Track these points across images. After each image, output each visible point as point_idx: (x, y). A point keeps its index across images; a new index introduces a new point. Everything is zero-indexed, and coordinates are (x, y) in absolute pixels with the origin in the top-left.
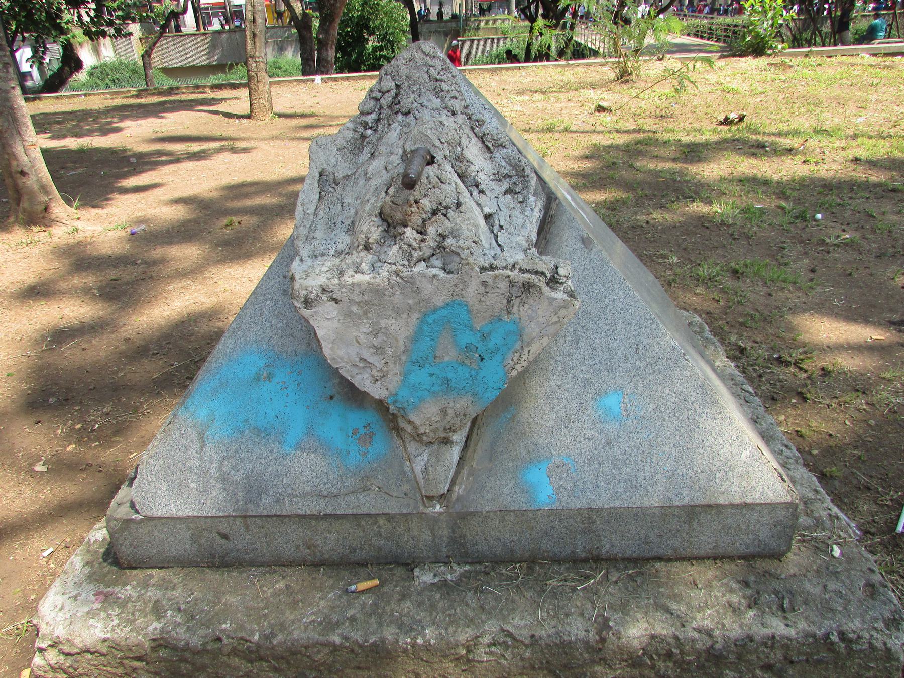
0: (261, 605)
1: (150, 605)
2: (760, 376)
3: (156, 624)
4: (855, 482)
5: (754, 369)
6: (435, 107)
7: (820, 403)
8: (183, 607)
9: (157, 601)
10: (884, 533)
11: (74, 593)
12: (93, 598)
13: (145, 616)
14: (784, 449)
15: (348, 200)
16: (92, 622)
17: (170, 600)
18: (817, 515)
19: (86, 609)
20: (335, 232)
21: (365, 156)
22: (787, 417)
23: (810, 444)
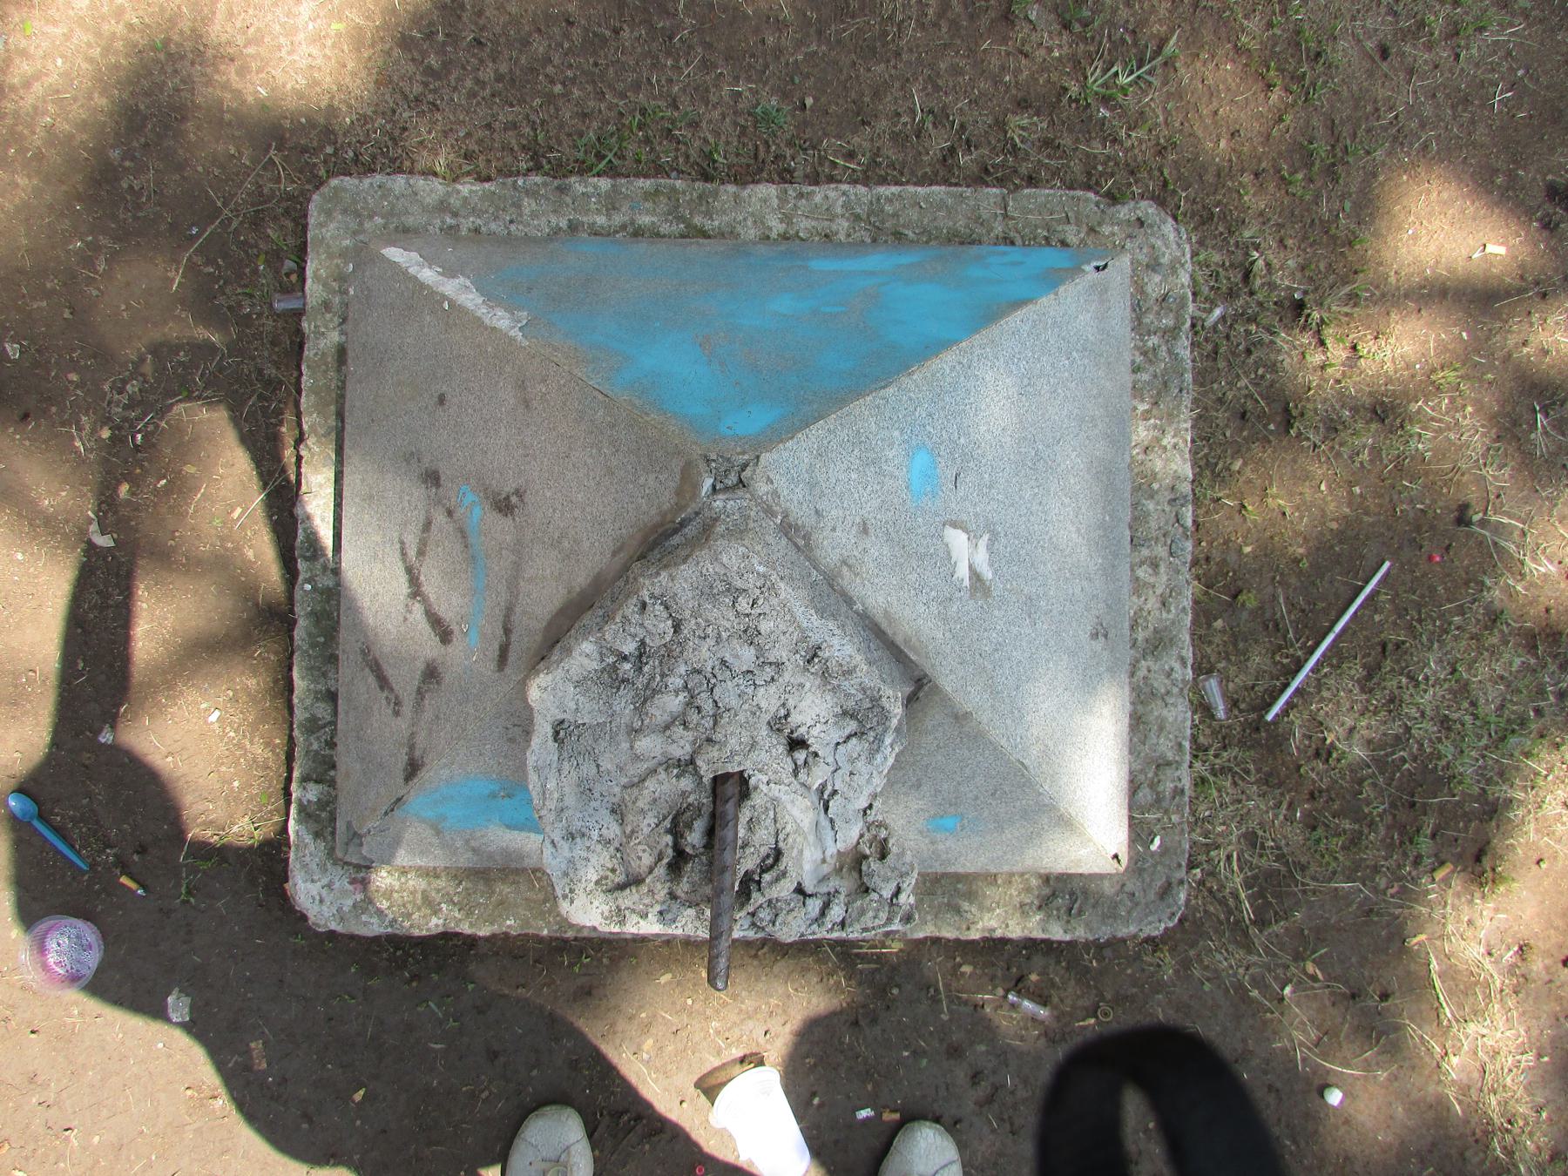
0: (541, 896)
1: (419, 896)
2: (1249, 352)
3: (434, 921)
4: (1268, 615)
5: (1248, 332)
6: (745, 668)
7: (1308, 439)
8: (456, 899)
9: (424, 892)
10: (1254, 709)
11: (325, 881)
12: (351, 888)
13: (419, 909)
14: (1177, 666)
15: (607, 764)
16: (364, 918)
17: (438, 891)
18: (1161, 788)
19: (350, 902)
20: (593, 804)
21: (623, 704)
22: (1245, 464)
23: (1249, 530)
